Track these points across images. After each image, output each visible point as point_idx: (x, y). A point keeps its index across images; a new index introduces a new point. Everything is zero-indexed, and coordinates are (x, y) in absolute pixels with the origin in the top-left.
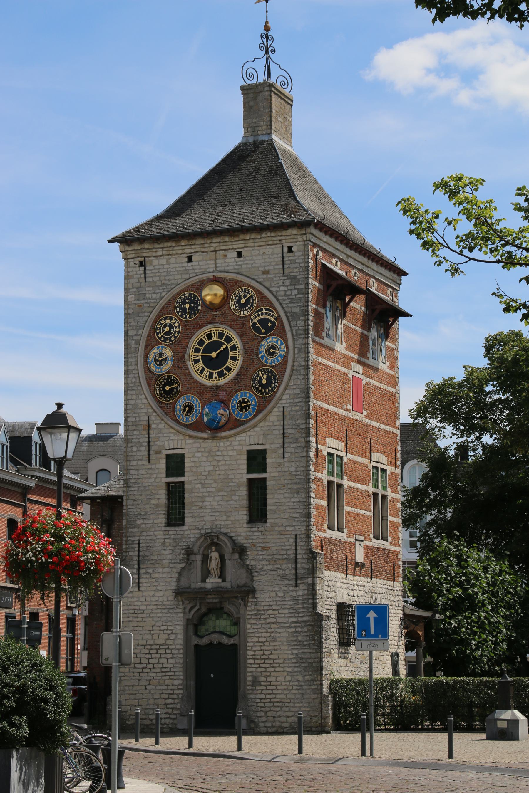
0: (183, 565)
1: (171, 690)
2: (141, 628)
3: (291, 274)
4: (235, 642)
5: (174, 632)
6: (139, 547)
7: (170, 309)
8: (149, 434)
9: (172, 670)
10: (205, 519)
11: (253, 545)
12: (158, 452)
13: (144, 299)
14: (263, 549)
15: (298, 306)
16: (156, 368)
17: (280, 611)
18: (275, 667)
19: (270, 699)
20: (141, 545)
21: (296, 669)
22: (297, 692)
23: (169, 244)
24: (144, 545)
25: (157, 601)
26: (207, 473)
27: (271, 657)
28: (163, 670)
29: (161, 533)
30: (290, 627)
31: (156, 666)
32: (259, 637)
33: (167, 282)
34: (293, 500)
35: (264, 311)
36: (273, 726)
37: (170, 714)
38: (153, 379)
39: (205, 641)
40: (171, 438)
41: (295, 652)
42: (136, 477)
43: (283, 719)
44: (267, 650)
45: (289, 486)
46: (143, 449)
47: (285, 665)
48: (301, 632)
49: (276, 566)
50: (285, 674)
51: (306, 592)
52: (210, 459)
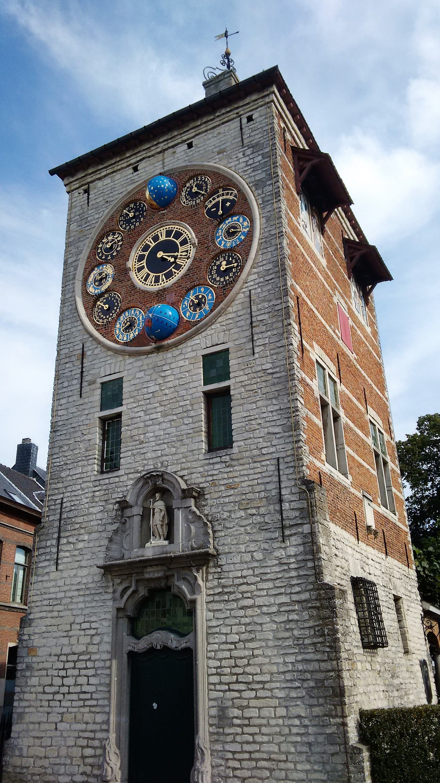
0: (115, 527)
1: (91, 731)
2: (55, 628)
3: (252, 143)
4: (188, 644)
5: (99, 631)
7: (112, 224)
8: (82, 363)
9: (94, 696)
11: (214, 483)
14: (230, 487)
15: (263, 171)
16: (95, 289)
17: (260, 586)
19: (250, 752)
20: (64, 505)
21: (293, 694)
22: (299, 739)
23: (113, 161)
24: (68, 504)
27: (248, 669)
28: (82, 696)
33: (112, 199)
34: (270, 408)
38: (91, 302)
39: (142, 645)
41: (291, 659)
42: (65, 418)
44: (242, 658)
45: (265, 390)
46: (75, 382)
47: (273, 685)
48: (298, 621)
49: (249, 511)
50: (276, 702)
51: (301, 548)
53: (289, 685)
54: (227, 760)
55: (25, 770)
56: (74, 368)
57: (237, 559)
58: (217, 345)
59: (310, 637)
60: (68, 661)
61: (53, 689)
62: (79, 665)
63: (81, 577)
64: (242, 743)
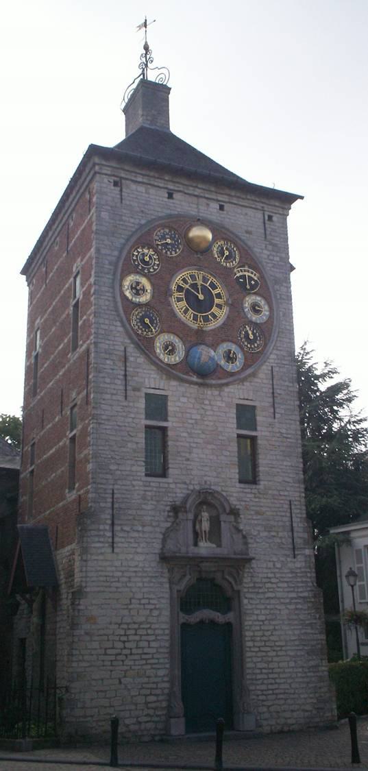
0: (169, 525)
1: (154, 683)
4: (230, 620)
6: (113, 498)
8: (126, 367)
9: (155, 656)
10: (194, 472)
11: (247, 508)
12: (136, 389)
13: (120, 221)
14: (258, 513)
17: (280, 585)
18: (277, 651)
19: (272, 690)
20: (115, 496)
21: (299, 653)
22: (301, 680)
23: (152, 174)
24: (119, 496)
25: (136, 566)
26: (193, 421)
27: (272, 638)
28: (144, 656)
29: (141, 483)
30: (290, 603)
31: (133, 651)
32: (257, 615)
33: (147, 211)
34: (285, 463)
35: (246, 268)
36: (278, 724)
37: (151, 716)
40: (152, 376)
41: (297, 632)
43: (288, 715)
44: (268, 631)
47: (289, 648)
52: (197, 406)
53: (297, 648)
54: (258, 696)
55: (89, 719)
56: (116, 367)
57: (265, 565)
58: (247, 399)
59: (308, 620)
60: (129, 629)
61: (114, 652)
62: (140, 632)
63: (138, 561)
64: (268, 684)
